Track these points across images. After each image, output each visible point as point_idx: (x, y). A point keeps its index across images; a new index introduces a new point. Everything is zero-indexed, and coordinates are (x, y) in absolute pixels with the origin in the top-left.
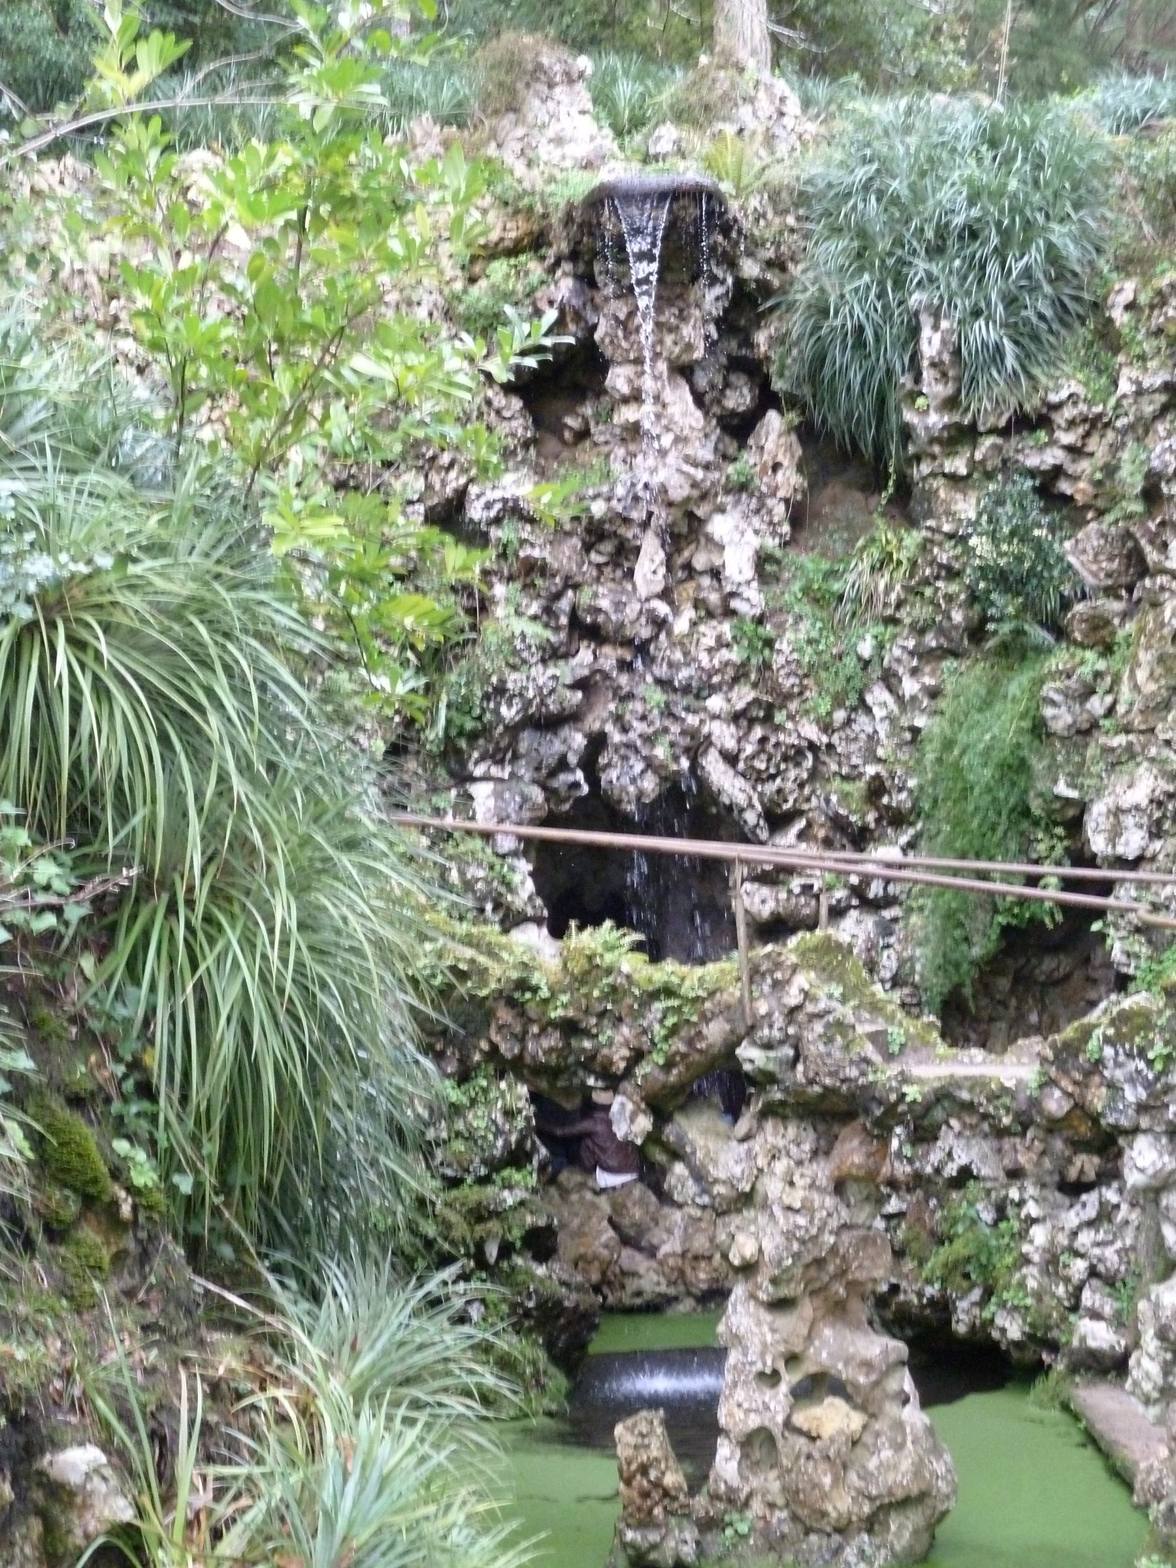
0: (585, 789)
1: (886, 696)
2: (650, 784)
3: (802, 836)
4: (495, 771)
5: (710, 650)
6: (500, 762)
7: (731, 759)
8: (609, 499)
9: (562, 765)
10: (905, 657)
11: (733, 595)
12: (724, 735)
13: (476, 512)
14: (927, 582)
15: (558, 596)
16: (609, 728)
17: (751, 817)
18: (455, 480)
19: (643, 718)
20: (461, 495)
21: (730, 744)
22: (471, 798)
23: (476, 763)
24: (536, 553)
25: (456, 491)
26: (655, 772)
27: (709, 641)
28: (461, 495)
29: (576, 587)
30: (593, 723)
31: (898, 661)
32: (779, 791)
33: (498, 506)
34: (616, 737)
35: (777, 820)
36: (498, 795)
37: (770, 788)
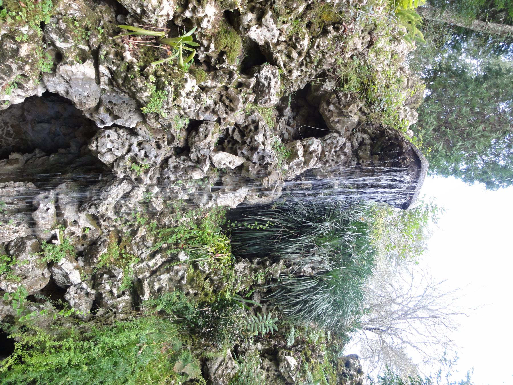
1: (159, 263)
2: (108, 159)
4: (104, 80)
8: (263, 143)
10: (178, 278)
14: (212, 280)
18: (281, 59)
19: (146, 155)
20: (274, 62)
22: (84, 61)
23: (108, 68)
24: (240, 105)
25: (276, 59)
26: (115, 161)
31: (177, 273)
36: (88, 80)
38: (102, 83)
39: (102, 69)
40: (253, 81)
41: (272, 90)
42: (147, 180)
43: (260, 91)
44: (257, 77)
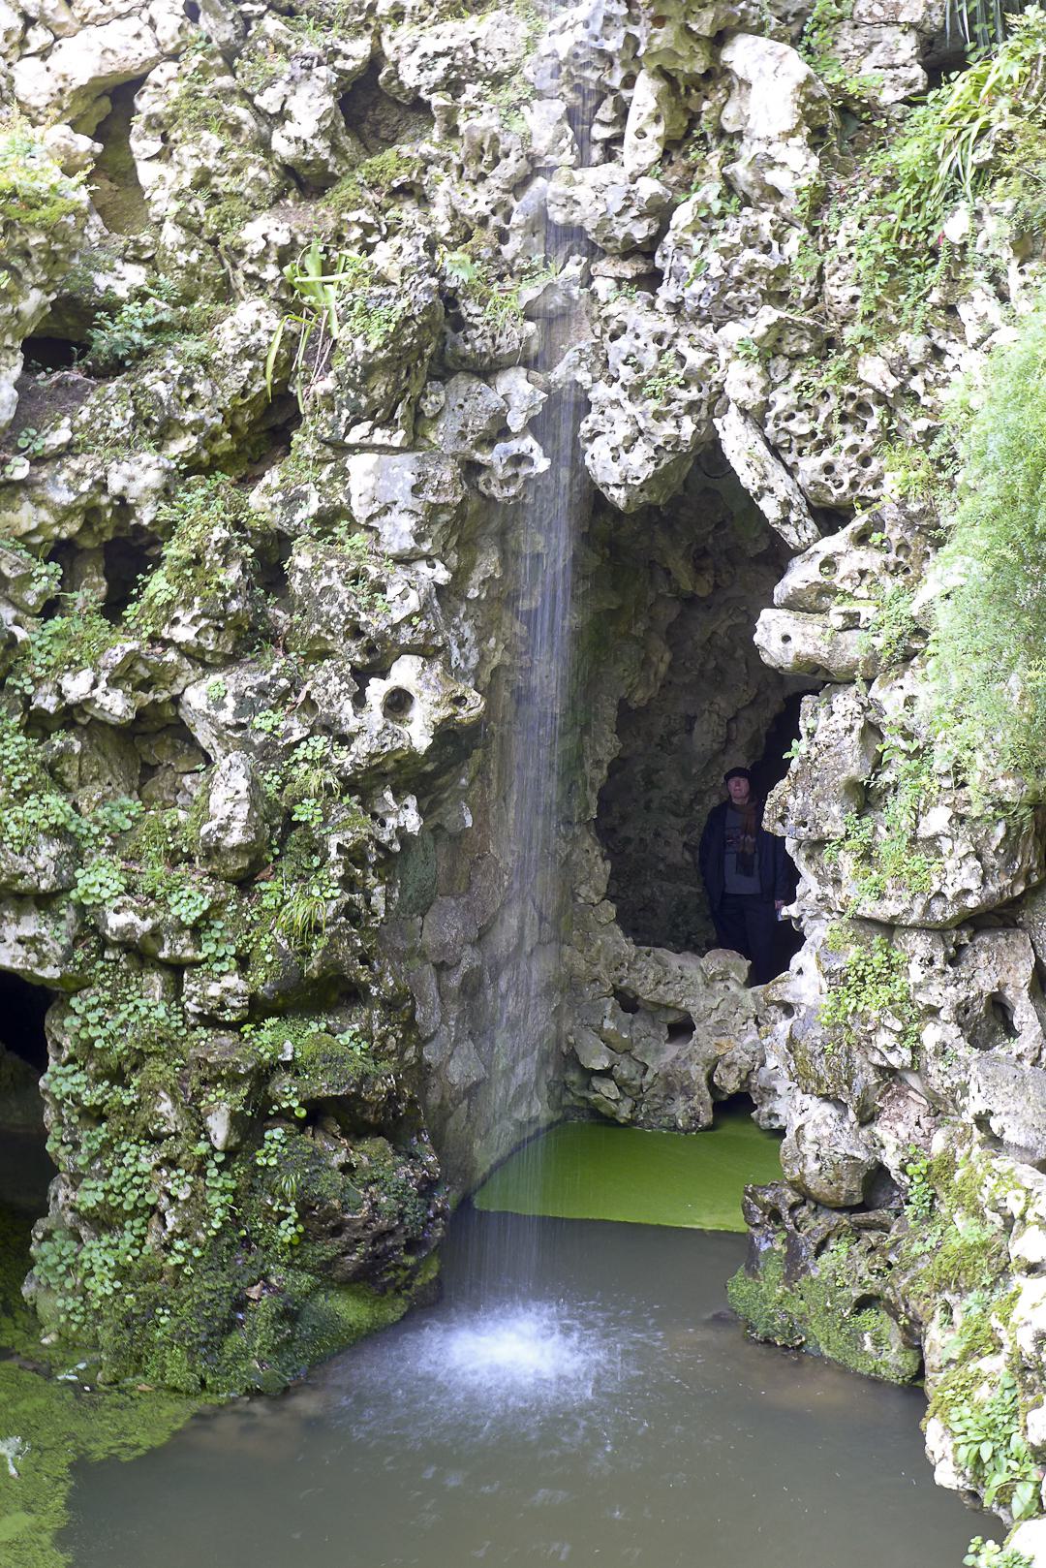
0: (542, 464)
3: (861, 539)
4: (380, 437)
5: (728, 252)
6: (388, 422)
7: (756, 416)
9: (500, 431)
12: (741, 381)
13: (409, 76)
16: (583, 377)
17: (770, 508)
21: (752, 397)
30: (559, 372)
32: (829, 469)
33: (445, 62)
34: (601, 392)
35: (830, 517)
36: (379, 472)
37: (810, 466)
38: (386, 441)
39: (353, 438)
40: (437, 100)
41: (454, 43)
42: (695, 359)
44: (431, 92)
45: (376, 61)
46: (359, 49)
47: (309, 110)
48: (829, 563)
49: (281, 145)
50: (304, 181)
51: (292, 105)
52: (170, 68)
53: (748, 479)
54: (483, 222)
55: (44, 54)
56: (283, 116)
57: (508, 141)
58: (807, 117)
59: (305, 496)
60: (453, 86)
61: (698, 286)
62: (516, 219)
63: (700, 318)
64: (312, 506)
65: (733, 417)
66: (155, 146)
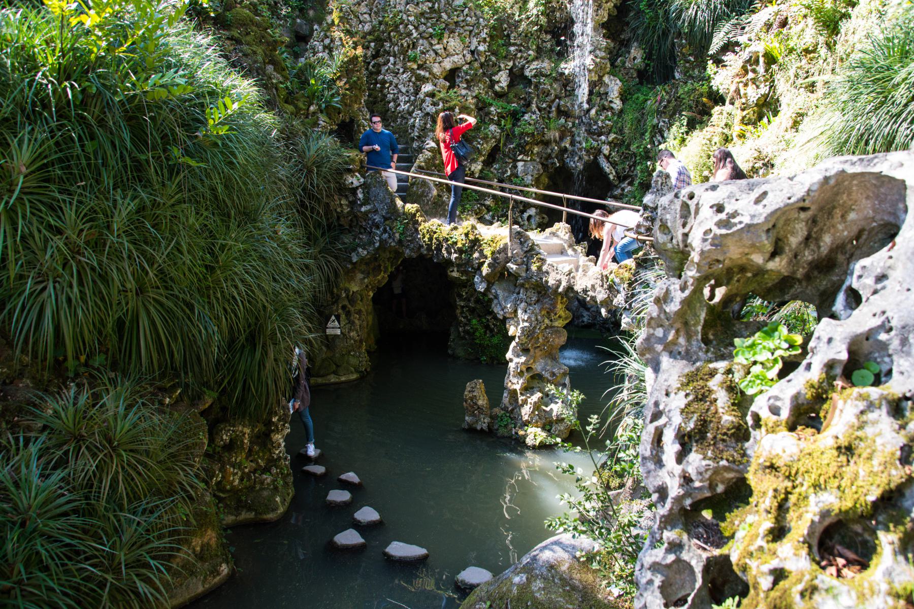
1: (660, 138)
3: (629, 184)
4: (525, 158)
6: (528, 156)
7: (607, 158)
11: (611, 102)
12: (606, 149)
13: (527, 73)
15: (553, 101)
16: (567, 146)
17: (611, 177)
20: (523, 66)
27: (602, 118)
28: (523, 66)
29: (560, 98)
36: (524, 166)
39: (519, 158)
40: (534, 80)
42: (595, 144)
43: (539, 74)
45: (514, 64)
46: (511, 64)
47: (503, 79)
48: (623, 189)
49: (496, 87)
50: (499, 96)
51: (502, 79)
52: (467, 66)
53: (607, 170)
54: (545, 109)
55: (440, 63)
56: (499, 82)
57: (552, 91)
58: (620, 94)
59: (507, 171)
60: (535, 76)
61: (595, 127)
62: (554, 109)
63: (594, 134)
64: (509, 173)
65: (602, 156)
66: (465, 86)
